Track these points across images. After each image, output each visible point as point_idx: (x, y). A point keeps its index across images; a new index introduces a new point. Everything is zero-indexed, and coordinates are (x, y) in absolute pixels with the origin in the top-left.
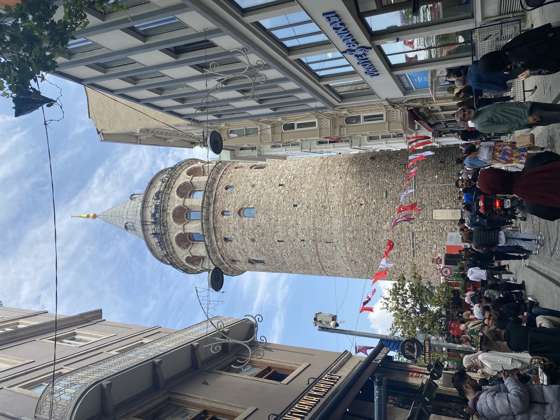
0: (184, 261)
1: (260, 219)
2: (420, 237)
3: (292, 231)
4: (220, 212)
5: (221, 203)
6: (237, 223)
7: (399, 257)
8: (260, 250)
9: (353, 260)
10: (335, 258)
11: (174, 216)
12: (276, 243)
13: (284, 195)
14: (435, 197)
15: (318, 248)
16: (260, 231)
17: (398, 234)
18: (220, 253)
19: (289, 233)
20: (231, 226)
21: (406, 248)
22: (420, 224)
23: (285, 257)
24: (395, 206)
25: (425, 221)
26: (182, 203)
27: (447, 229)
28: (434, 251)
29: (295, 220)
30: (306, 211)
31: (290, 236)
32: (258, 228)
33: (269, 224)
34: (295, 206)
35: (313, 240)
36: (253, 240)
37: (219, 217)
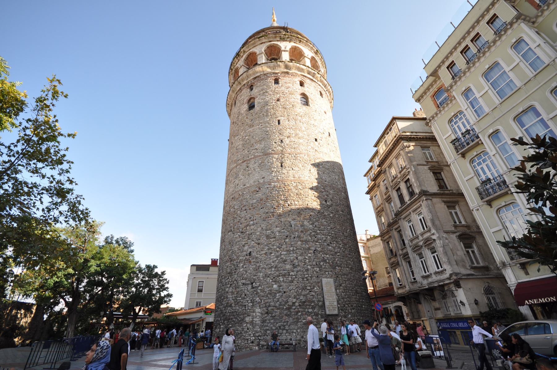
0: (251, 51)
2: (298, 262)
7: (268, 237)
9: (260, 188)
10: (262, 171)
14: (344, 282)
17: (299, 237)
19: (289, 130)
21: (282, 245)
22: (314, 263)
23: (260, 126)
24: (329, 236)
25: (318, 269)
27: (312, 295)
28: (282, 279)
34: (316, 140)
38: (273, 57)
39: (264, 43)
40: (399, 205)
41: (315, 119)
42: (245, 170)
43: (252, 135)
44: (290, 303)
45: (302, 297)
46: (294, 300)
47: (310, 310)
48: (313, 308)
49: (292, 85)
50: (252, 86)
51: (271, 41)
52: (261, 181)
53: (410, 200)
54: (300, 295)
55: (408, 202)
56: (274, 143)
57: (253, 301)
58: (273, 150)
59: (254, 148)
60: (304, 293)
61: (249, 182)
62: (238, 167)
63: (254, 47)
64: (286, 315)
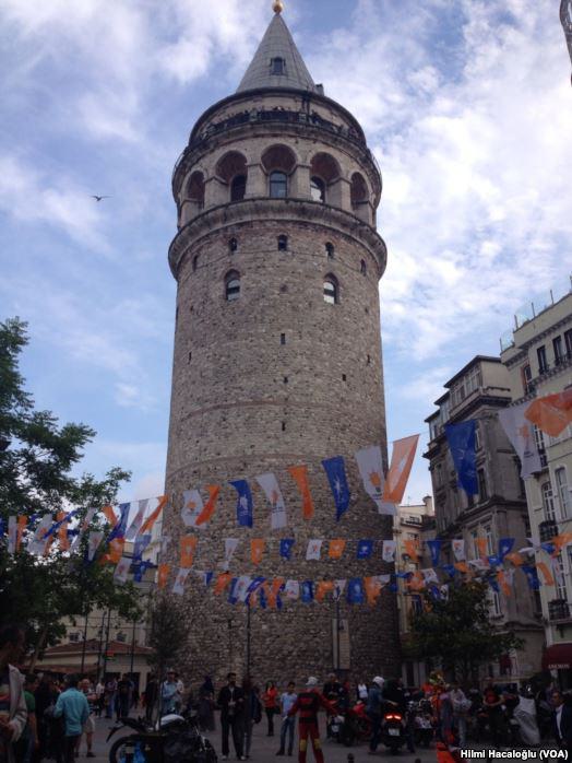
0: (233, 148)
8: (263, 297)
11: (325, 155)
12: (279, 329)
16: (300, 305)
19: (299, 357)
23: (248, 341)
27: (317, 642)
30: (337, 394)
34: (344, 377)
35: (286, 399)
36: (284, 289)
37: (325, 238)
38: (279, 169)
39: (263, 136)
40: (466, 505)
42: (219, 424)
43: (233, 356)
44: (285, 652)
45: (302, 644)
46: (291, 648)
47: (312, 663)
48: (317, 660)
50: (233, 240)
51: (275, 136)
52: (249, 452)
53: (479, 503)
54: (299, 641)
55: (478, 506)
56: (272, 383)
57: (230, 647)
59: (238, 385)
60: (306, 638)
61: (226, 449)
62: (205, 414)
63: (241, 139)
64: (279, 668)
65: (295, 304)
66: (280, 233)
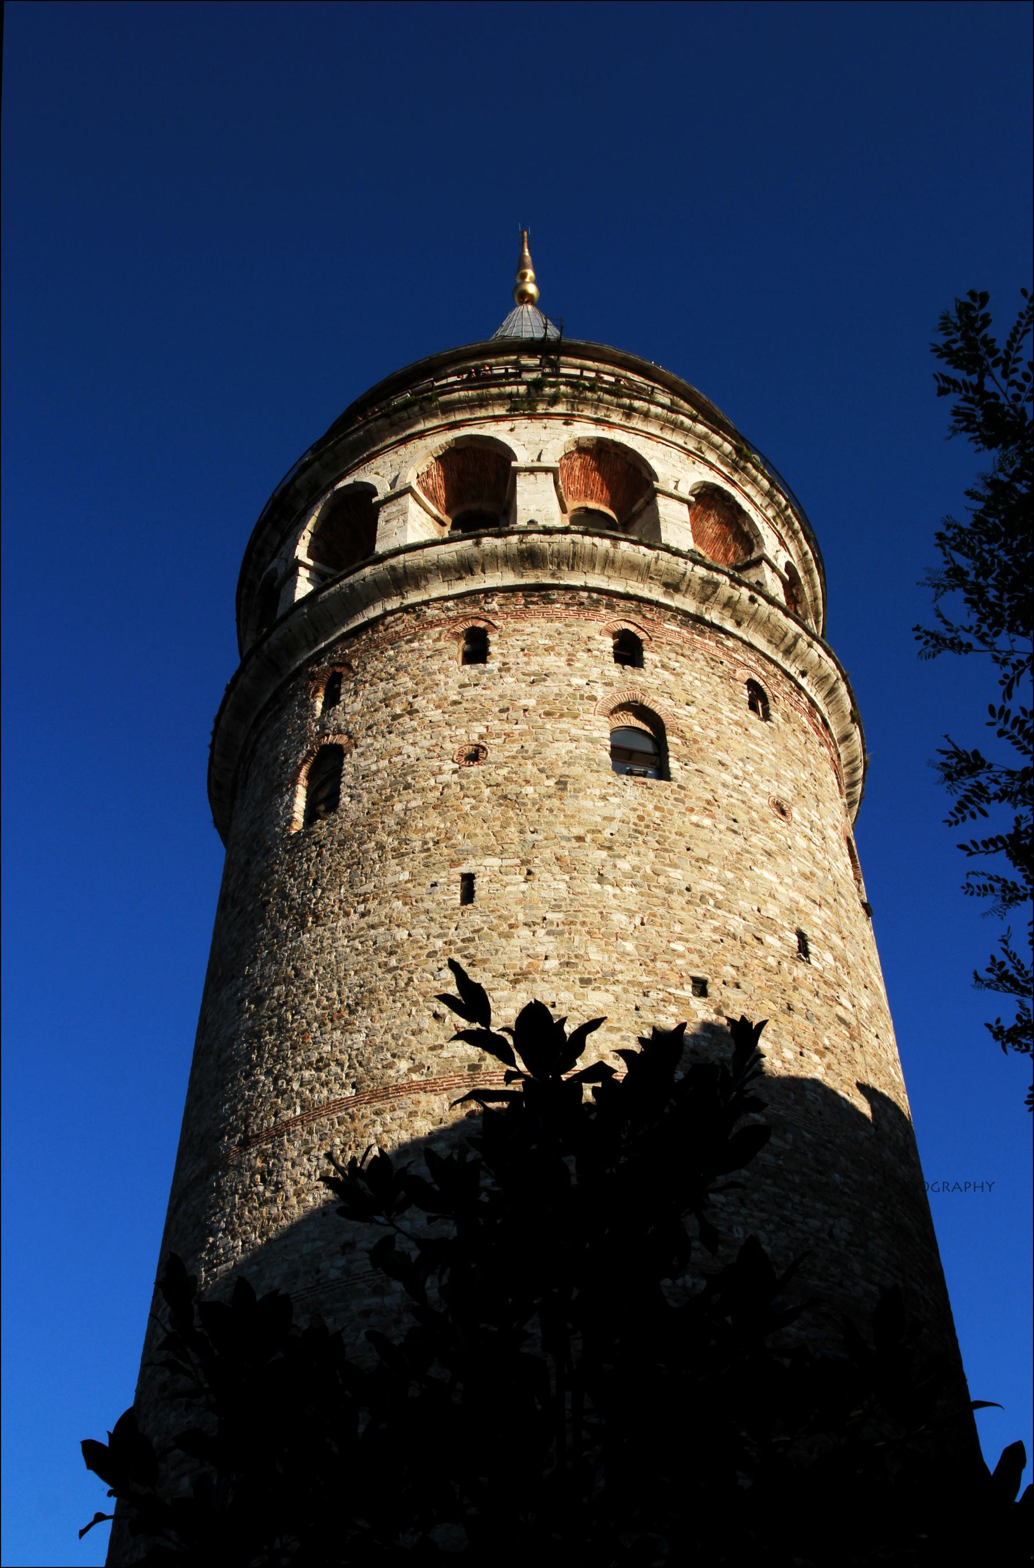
1: (604, 798)
3: (541, 950)
4: (632, 628)
5: (679, 642)
6: (578, 688)
8: (407, 787)
12: (454, 863)
13: (755, 942)
15: (422, 1097)
16: (529, 790)
18: (392, 612)
19: (525, 932)
20: (553, 662)
26: (670, 488)
29: (609, 977)
31: (508, 936)
32: (551, 783)
33: (580, 839)
34: (700, 987)
38: (474, 506)
41: (700, 852)
49: (562, 662)
58: (417, 1068)
65: (511, 789)
66: (470, 624)
